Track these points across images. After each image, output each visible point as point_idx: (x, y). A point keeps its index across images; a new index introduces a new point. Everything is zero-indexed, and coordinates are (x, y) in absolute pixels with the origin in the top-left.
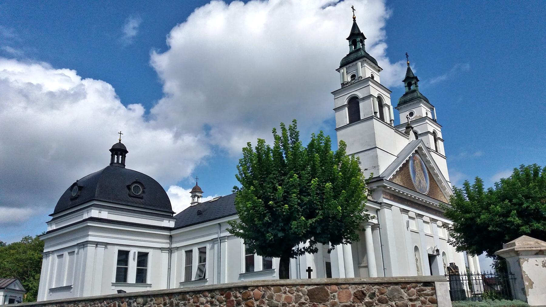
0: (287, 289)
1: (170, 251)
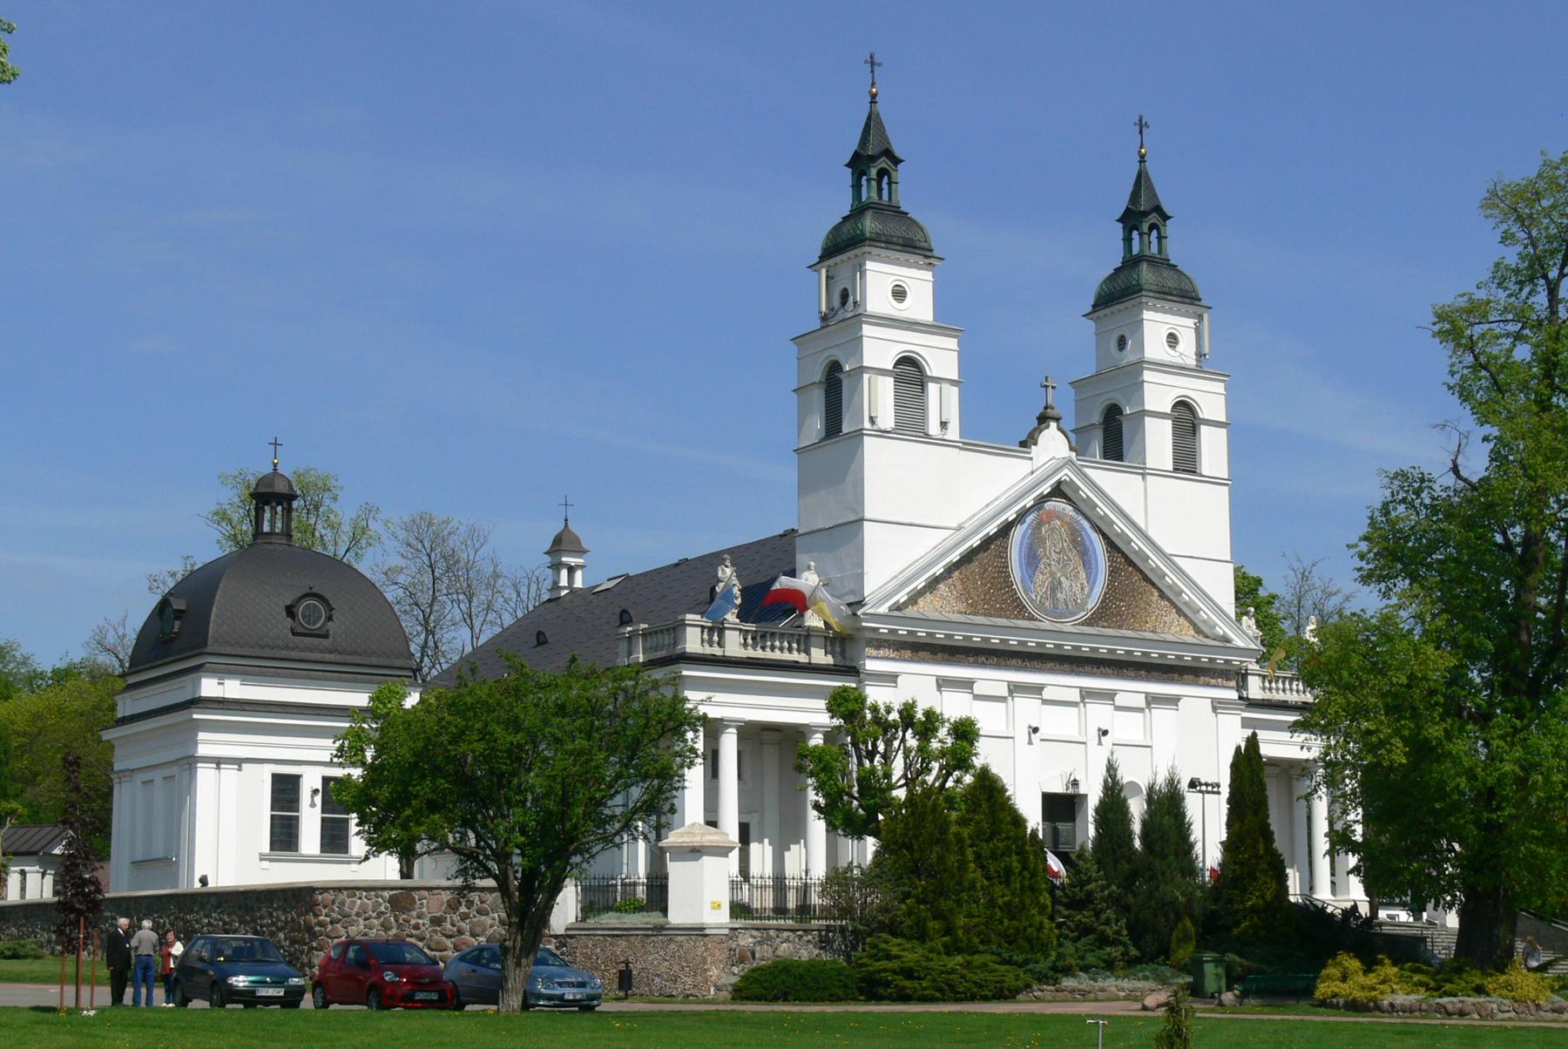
0: (364, 893)
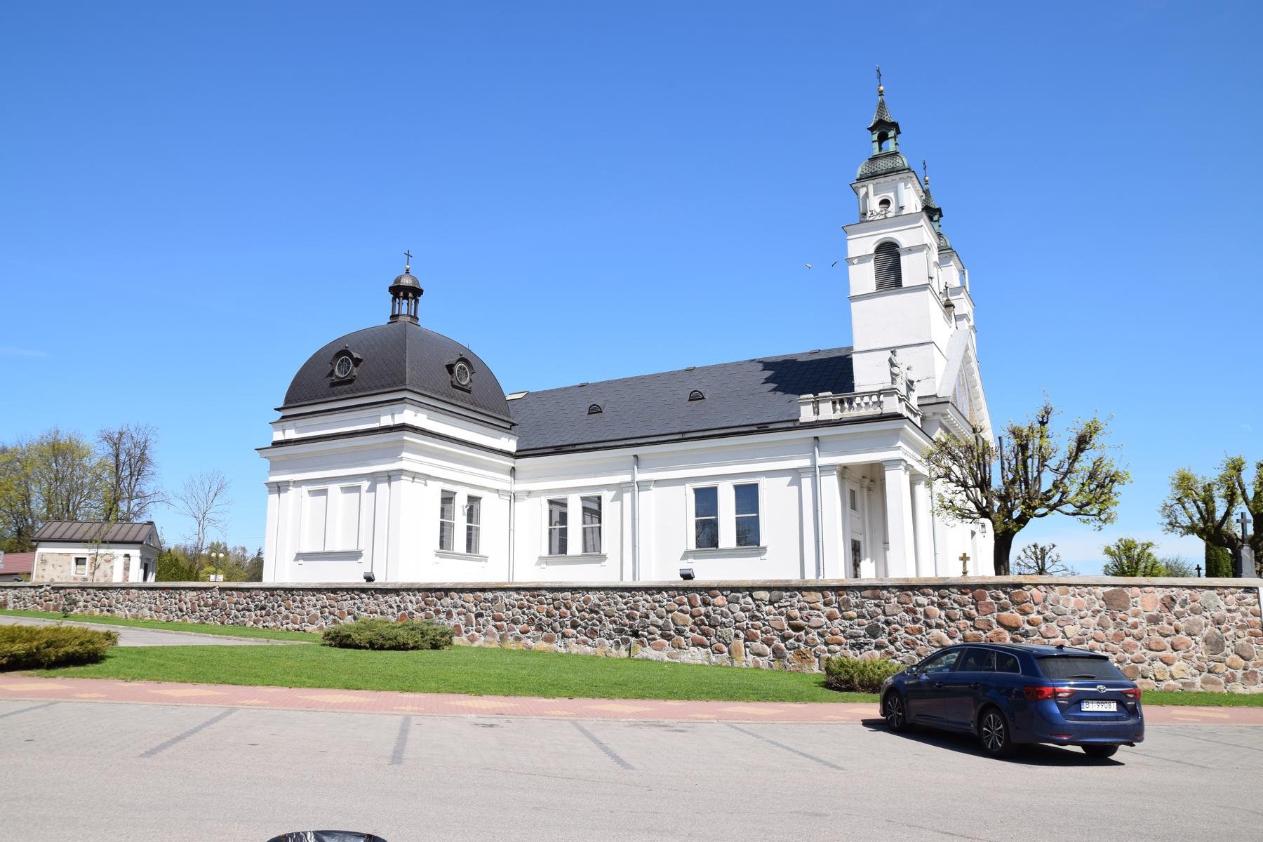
1: (513, 497)
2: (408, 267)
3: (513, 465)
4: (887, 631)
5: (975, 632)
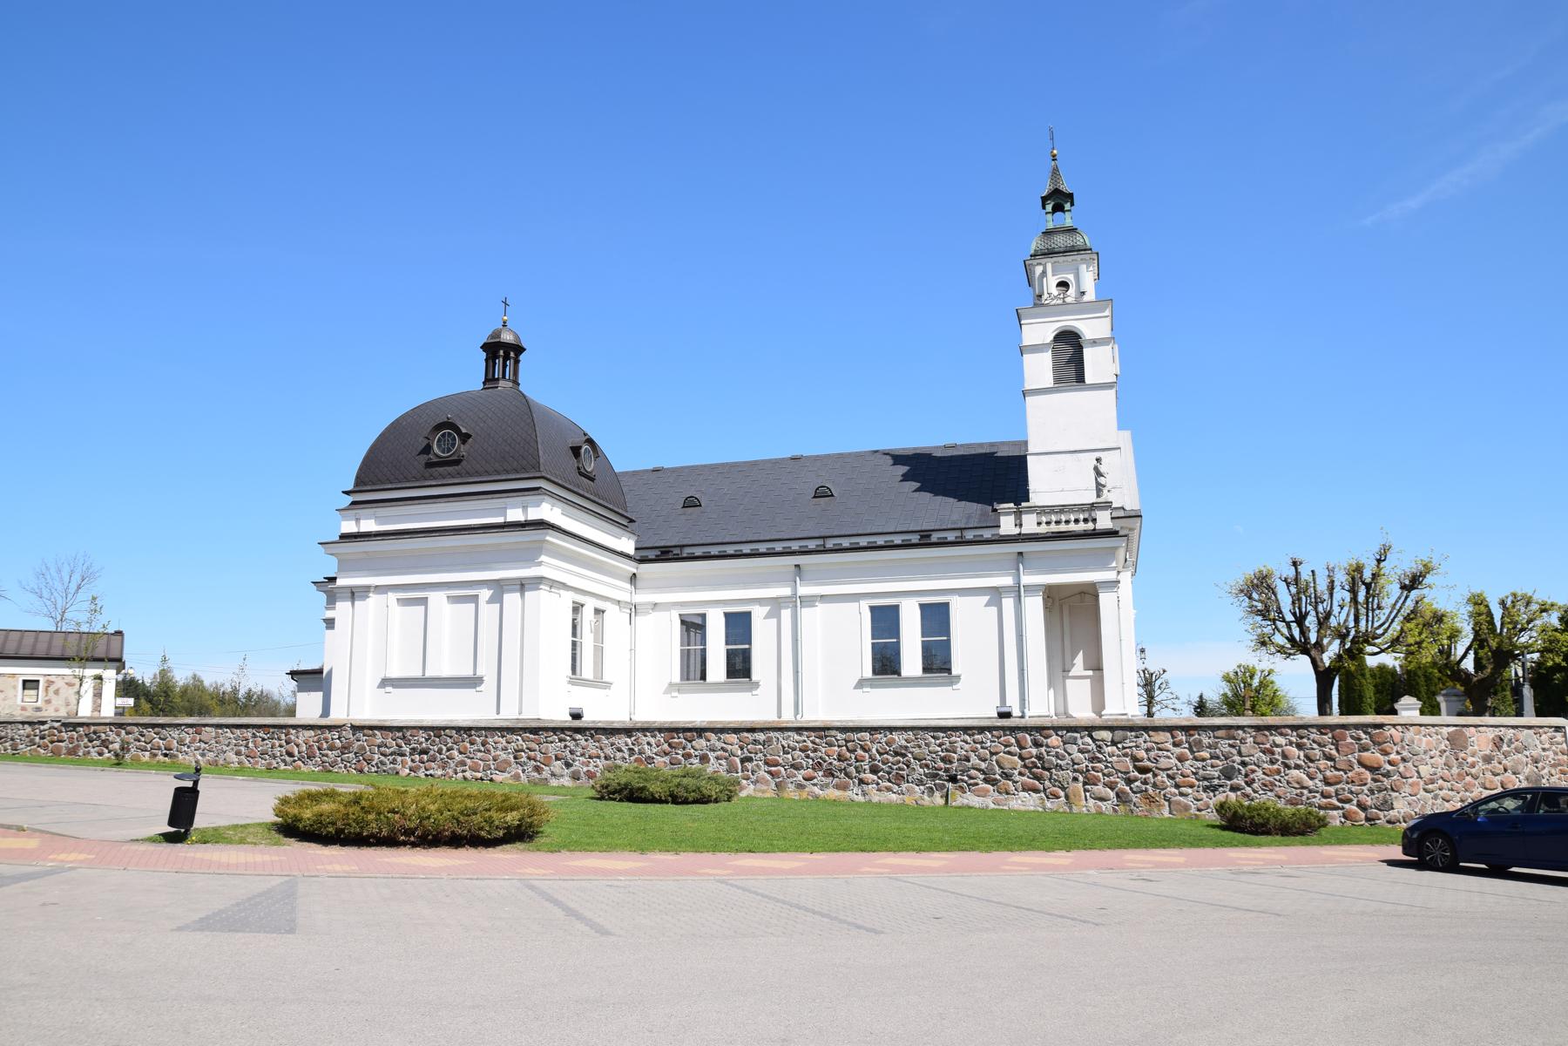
1: (633, 610)
2: (505, 318)
3: (635, 571)
4: (1243, 772)
5: (1337, 773)
